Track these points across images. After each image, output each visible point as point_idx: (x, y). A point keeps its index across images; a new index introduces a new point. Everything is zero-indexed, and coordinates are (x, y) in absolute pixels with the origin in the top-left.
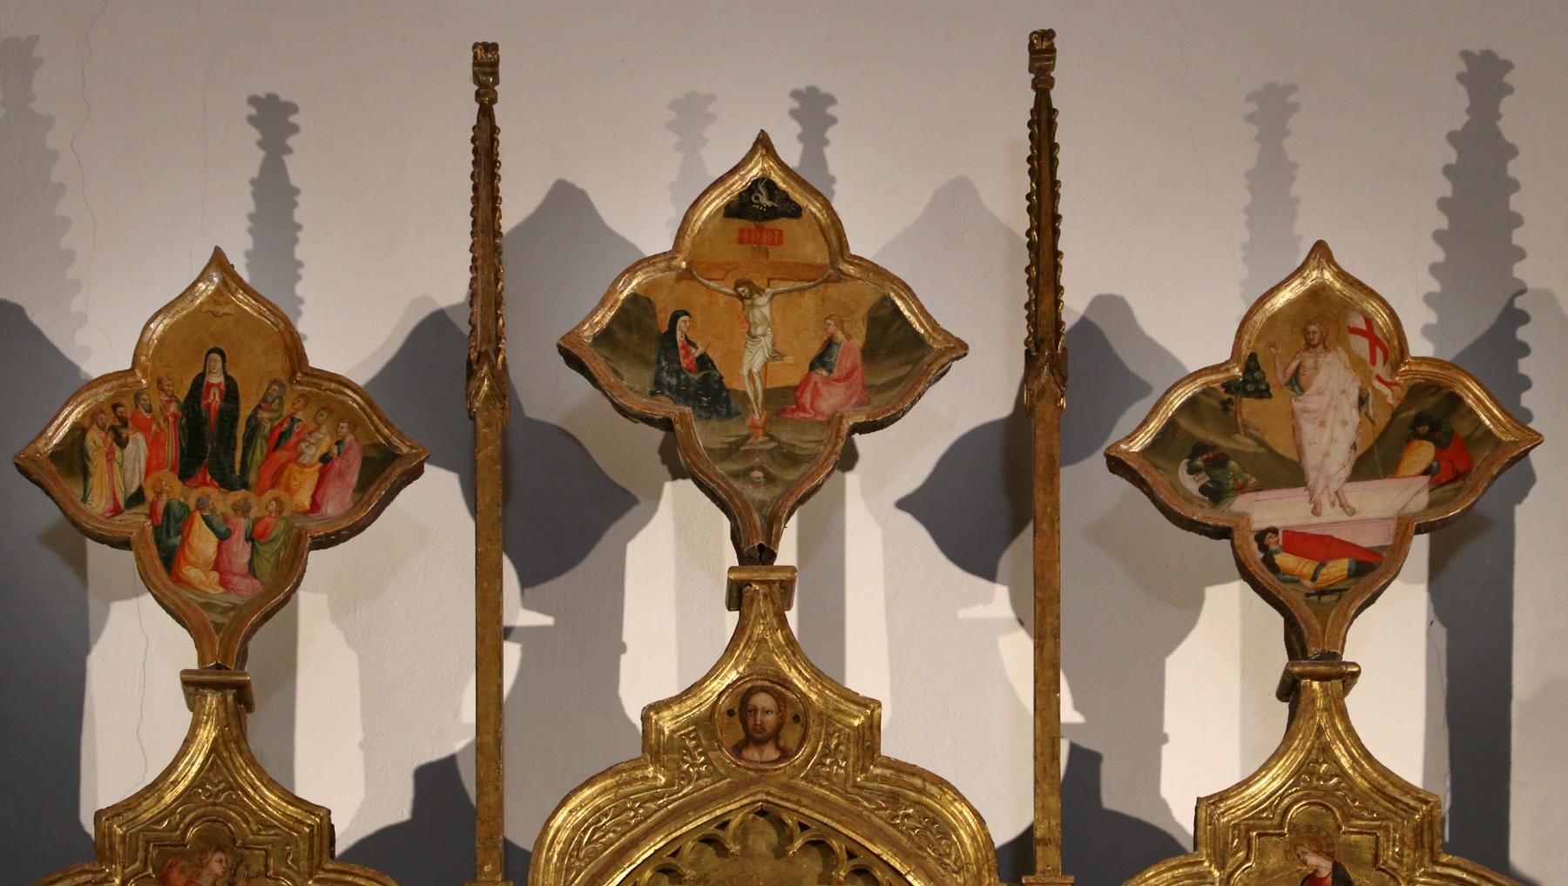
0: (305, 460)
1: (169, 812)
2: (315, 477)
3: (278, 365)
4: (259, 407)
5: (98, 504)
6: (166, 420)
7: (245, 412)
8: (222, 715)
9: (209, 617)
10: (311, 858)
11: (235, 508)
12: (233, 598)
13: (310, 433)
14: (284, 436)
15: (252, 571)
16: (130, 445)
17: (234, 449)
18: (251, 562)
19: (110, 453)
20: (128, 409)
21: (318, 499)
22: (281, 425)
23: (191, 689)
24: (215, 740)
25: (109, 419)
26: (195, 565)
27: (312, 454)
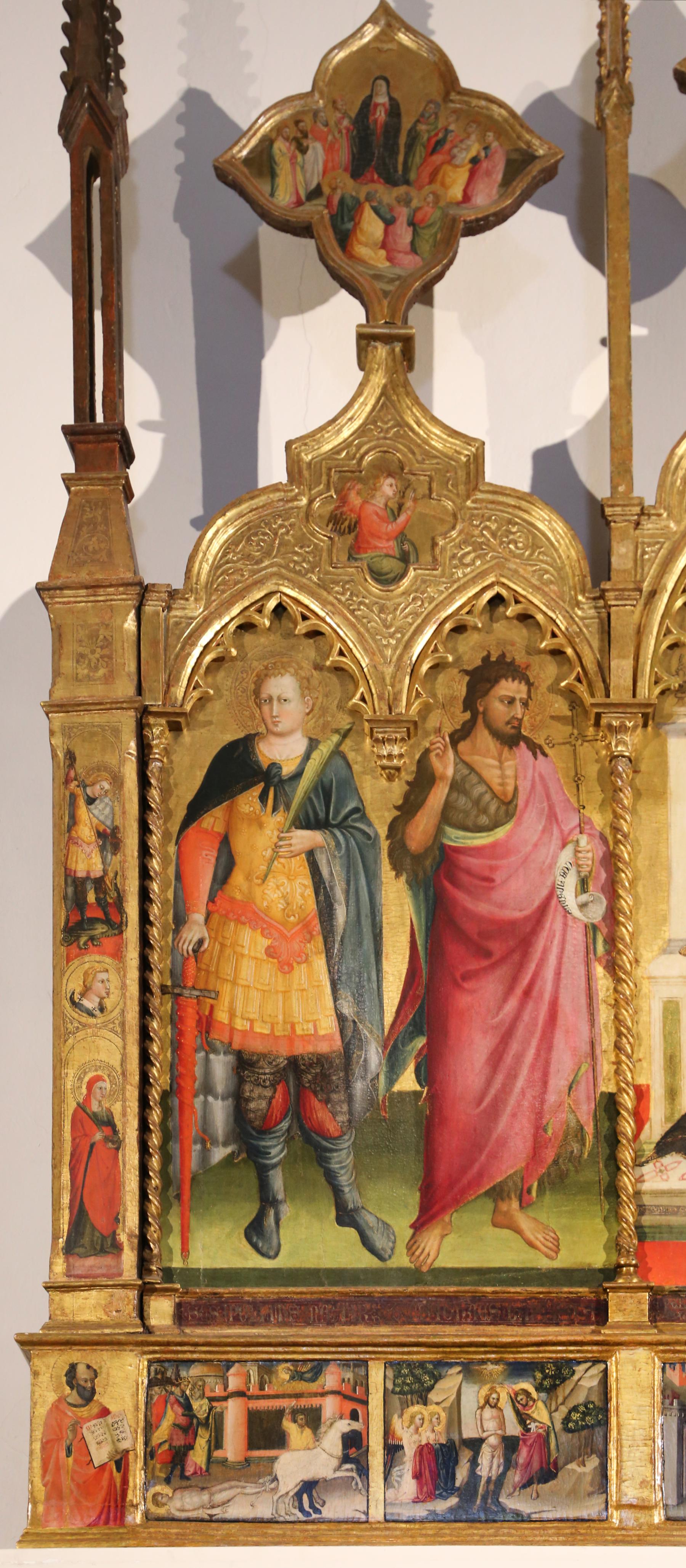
0: (457, 161)
1: (347, 444)
2: (466, 175)
3: (435, 88)
4: (418, 121)
5: (284, 197)
6: (340, 132)
7: (406, 124)
8: (390, 364)
9: (380, 285)
10: (468, 481)
11: (398, 200)
12: (398, 271)
13: (462, 141)
14: (440, 143)
15: (414, 249)
16: (310, 152)
17: (397, 153)
18: (412, 243)
19: (293, 159)
20: (307, 123)
21: (469, 193)
22: (437, 135)
23: (364, 342)
24: (385, 386)
25: (291, 132)
26: (366, 245)
27: (464, 157)
